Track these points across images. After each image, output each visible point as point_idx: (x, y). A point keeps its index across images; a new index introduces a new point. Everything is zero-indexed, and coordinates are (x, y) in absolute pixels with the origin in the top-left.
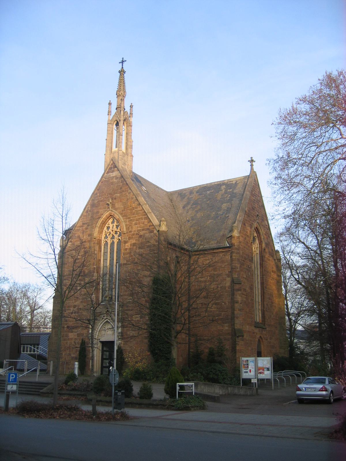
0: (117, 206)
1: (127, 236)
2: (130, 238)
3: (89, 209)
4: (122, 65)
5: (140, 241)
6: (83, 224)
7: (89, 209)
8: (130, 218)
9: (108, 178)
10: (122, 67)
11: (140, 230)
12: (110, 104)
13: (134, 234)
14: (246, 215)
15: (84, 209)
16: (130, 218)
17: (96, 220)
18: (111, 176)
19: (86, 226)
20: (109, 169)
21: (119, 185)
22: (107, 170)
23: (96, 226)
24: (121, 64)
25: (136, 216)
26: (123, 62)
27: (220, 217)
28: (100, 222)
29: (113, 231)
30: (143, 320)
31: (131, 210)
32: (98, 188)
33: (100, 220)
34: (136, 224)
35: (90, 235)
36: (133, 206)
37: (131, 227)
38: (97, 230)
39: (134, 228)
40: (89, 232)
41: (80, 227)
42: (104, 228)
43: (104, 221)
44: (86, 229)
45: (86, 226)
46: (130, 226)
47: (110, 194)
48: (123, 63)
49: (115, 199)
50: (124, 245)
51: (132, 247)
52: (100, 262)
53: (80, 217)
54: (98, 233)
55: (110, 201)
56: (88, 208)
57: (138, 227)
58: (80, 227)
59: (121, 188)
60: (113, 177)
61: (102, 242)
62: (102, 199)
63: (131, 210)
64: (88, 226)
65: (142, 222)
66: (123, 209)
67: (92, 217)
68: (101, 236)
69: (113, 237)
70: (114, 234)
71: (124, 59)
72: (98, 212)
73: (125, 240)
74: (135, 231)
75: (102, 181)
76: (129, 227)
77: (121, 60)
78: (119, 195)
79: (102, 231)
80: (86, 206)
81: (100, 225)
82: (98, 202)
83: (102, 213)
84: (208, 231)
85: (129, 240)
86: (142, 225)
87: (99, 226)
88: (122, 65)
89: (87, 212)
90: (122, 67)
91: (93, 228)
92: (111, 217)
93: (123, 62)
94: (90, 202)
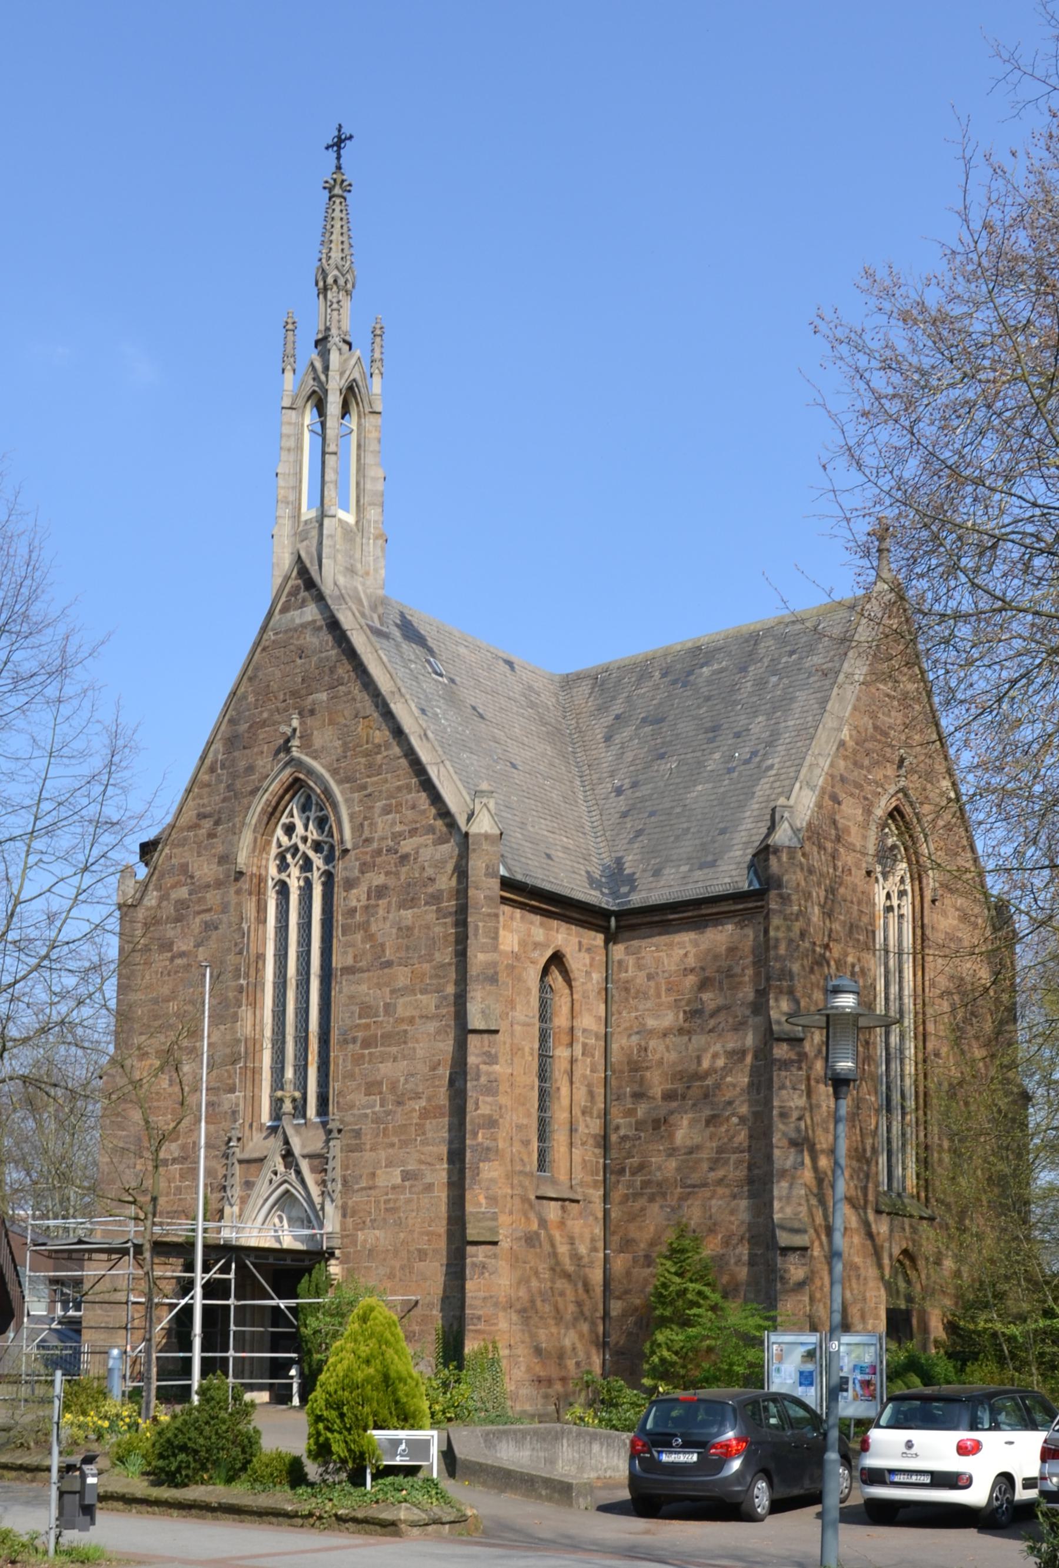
0: (318, 741)
1: (357, 859)
2: (364, 868)
3: (220, 757)
4: (339, 158)
5: (403, 877)
6: (202, 816)
7: (220, 757)
8: (364, 787)
9: (286, 632)
10: (339, 168)
11: (400, 834)
12: (290, 327)
13: (379, 852)
14: (845, 758)
15: (203, 759)
16: (364, 787)
17: (245, 801)
18: (298, 621)
19: (207, 824)
20: (290, 594)
21: (328, 659)
22: (283, 599)
23: (243, 824)
24: (332, 154)
25: (386, 781)
26: (339, 143)
27: (740, 773)
28: (259, 809)
29: (305, 840)
30: (411, 1187)
31: (367, 754)
32: (250, 673)
33: (256, 801)
34: (387, 811)
35: (225, 859)
36: (376, 741)
37: (371, 824)
38: (247, 838)
39: (380, 825)
40: (220, 849)
41: (190, 828)
42: (274, 831)
43: (273, 803)
44: (211, 835)
45: (207, 824)
46: (365, 818)
47: (294, 694)
48: (339, 148)
49: (312, 712)
50: (344, 894)
51: (372, 902)
52: (260, 963)
53: (189, 791)
54: (254, 850)
55: (295, 723)
56: (216, 752)
57: (393, 823)
58: (190, 828)
59: (332, 670)
60: (304, 626)
61: (270, 883)
62: (265, 715)
63: (367, 754)
64: (217, 823)
65: (410, 803)
66: (339, 751)
67: (229, 787)
68: (264, 862)
69: (307, 865)
70: (311, 854)
71: (346, 131)
72: (250, 769)
73: (348, 874)
74: (382, 839)
75: (263, 643)
76: (362, 825)
77: (329, 138)
78: (323, 696)
79: (268, 843)
80: (210, 744)
81: (259, 821)
82: (250, 727)
83: (264, 771)
84: (688, 829)
85: (363, 873)
86: (410, 814)
87: (254, 821)
88: (339, 158)
89: (212, 770)
90: (339, 168)
91: (235, 832)
92: (297, 786)
93: (339, 143)
94: (223, 727)
